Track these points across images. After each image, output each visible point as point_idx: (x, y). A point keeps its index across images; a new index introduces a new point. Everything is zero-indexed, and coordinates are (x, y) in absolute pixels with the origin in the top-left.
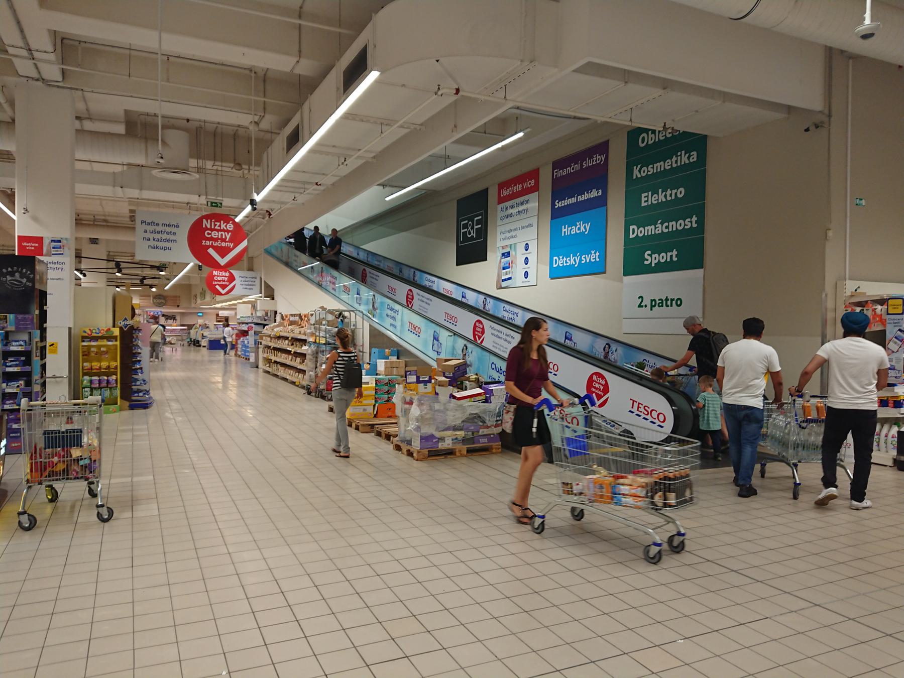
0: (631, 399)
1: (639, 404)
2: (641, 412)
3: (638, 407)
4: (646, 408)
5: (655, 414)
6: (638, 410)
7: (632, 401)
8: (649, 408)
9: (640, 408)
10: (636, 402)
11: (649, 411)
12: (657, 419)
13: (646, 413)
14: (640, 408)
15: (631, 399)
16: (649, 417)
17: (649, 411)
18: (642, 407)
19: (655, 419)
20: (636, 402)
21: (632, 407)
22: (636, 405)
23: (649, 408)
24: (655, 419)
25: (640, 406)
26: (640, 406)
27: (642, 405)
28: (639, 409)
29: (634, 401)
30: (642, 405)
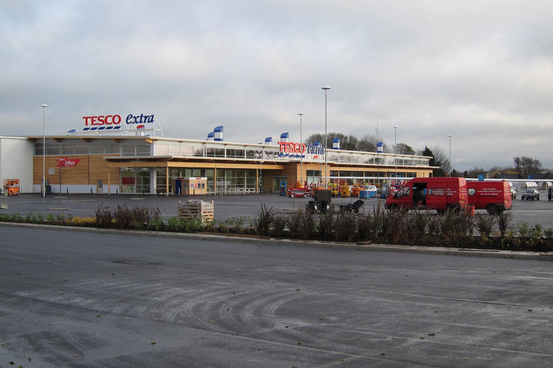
0: (84, 118)
1: (93, 118)
2: (96, 124)
3: (93, 121)
4: (101, 118)
5: (110, 120)
6: (92, 124)
7: (85, 119)
8: (103, 117)
9: (95, 121)
10: (89, 118)
11: (104, 119)
12: (112, 123)
13: (101, 123)
14: (95, 121)
15: (84, 118)
16: (106, 126)
17: (104, 120)
18: (97, 119)
19: (111, 123)
20: (89, 118)
21: (87, 124)
23: (103, 117)
24: (111, 123)
26: (94, 119)
27: (96, 117)
29: (87, 118)
30: (96, 117)
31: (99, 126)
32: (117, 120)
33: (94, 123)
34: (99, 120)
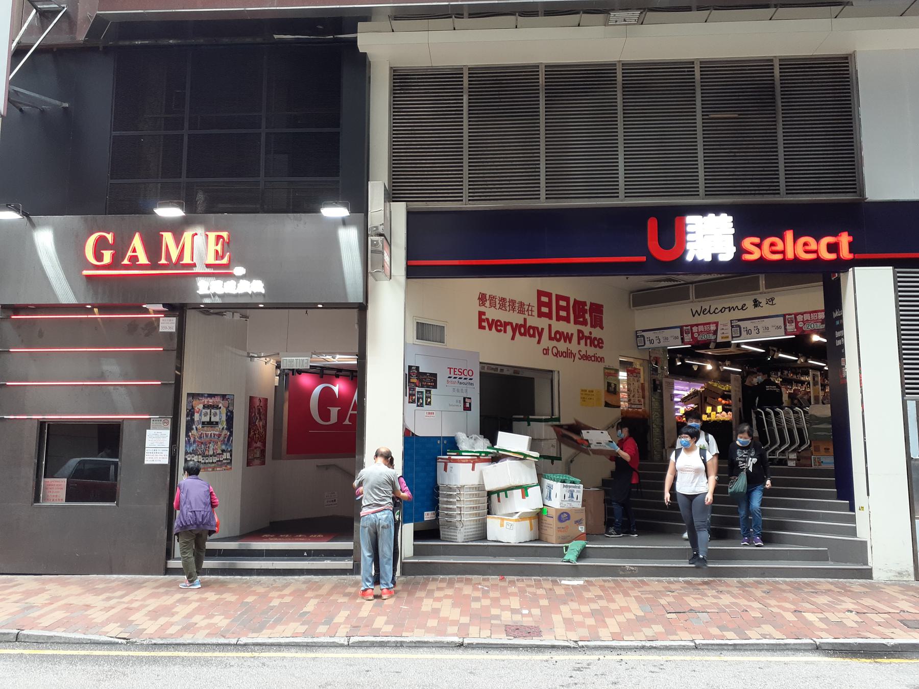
1: (454, 369)
3: (454, 371)
4: (460, 370)
5: (466, 373)
6: (454, 374)
8: (461, 369)
13: (460, 374)
16: (463, 376)
21: (450, 373)
22: (452, 370)
23: (461, 369)
25: (456, 370)
26: (456, 370)
28: (456, 373)
29: (450, 368)
31: (459, 377)
32: (470, 373)
33: (456, 373)
34: (459, 372)
